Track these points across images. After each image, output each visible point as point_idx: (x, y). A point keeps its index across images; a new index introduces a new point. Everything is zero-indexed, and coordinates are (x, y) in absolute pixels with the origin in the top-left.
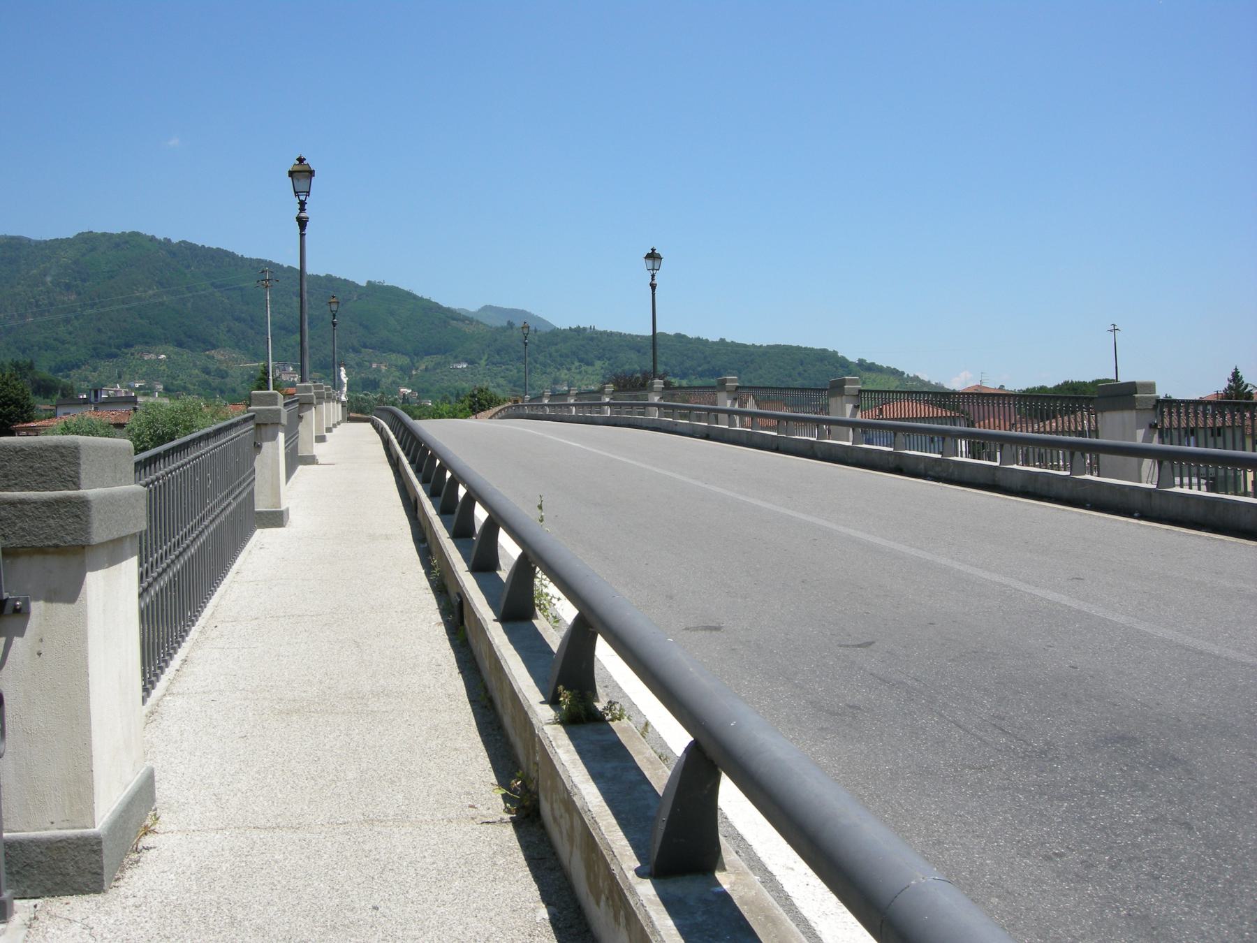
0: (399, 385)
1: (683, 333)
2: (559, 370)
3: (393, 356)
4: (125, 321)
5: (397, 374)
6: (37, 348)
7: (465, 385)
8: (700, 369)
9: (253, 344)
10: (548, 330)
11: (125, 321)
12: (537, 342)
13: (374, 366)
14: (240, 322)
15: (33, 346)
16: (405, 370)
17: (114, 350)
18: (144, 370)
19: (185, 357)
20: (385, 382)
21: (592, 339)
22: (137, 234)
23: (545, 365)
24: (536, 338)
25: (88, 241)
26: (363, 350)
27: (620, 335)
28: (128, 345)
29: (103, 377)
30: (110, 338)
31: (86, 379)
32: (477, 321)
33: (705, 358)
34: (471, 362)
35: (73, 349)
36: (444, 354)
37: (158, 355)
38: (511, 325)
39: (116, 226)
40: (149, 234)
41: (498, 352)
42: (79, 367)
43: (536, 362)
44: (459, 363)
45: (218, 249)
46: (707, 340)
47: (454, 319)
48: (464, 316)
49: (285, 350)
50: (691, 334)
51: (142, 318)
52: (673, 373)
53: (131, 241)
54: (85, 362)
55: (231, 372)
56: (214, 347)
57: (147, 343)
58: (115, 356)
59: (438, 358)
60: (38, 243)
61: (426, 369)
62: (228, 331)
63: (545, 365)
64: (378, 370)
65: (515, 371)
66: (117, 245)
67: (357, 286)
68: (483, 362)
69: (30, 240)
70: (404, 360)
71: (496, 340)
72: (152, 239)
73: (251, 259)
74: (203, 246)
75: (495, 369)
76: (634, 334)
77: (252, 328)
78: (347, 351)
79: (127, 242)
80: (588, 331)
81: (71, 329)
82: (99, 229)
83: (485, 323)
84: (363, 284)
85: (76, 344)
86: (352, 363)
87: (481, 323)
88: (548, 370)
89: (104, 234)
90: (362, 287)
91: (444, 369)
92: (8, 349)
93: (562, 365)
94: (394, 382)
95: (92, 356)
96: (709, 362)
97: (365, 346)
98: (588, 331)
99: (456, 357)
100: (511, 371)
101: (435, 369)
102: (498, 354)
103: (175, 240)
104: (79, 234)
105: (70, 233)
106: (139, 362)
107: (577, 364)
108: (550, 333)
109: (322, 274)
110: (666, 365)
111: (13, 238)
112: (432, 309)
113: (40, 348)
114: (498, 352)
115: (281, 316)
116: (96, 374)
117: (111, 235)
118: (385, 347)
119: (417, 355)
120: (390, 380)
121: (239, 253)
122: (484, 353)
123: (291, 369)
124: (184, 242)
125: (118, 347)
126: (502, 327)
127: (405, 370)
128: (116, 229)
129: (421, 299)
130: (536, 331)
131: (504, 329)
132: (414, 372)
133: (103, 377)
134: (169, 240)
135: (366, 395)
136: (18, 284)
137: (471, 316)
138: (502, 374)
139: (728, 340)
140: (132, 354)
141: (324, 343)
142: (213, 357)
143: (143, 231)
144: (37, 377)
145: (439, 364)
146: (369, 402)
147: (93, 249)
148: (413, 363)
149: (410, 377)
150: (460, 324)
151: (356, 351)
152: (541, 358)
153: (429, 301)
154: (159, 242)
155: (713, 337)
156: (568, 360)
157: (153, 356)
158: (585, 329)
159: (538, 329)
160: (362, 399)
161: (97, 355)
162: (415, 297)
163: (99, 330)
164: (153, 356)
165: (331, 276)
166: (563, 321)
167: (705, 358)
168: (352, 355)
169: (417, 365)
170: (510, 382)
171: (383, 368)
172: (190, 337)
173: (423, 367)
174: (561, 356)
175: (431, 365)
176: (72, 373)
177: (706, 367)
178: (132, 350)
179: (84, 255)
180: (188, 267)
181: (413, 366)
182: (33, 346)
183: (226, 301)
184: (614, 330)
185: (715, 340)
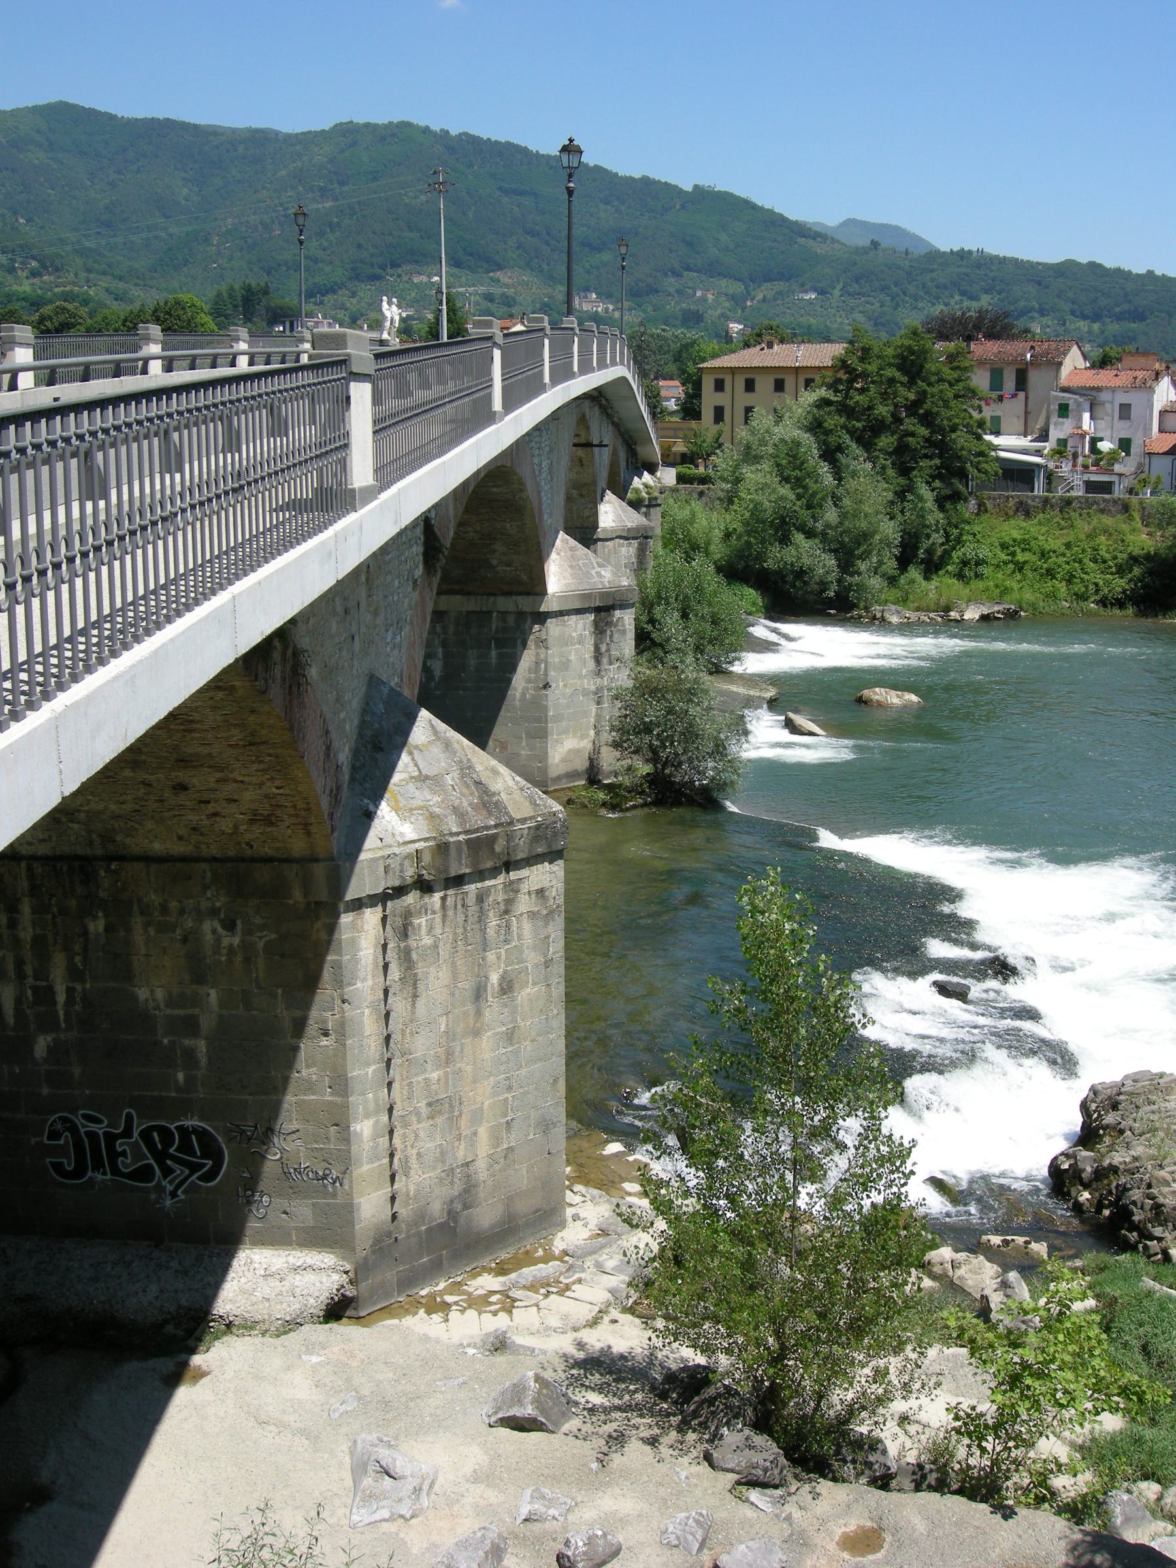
0: (728, 319)
1: (1098, 261)
2: (934, 304)
3: (723, 282)
4: (390, 234)
5: (727, 304)
6: (284, 268)
7: (812, 321)
8: (1117, 310)
9: (548, 264)
10: (924, 251)
11: (390, 234)
12: (907, 268)
13: (699, 294)
14: (533, 236)
15: (279, 265)
16: (738, 301)
17: (378, 271)
18: (413, 295)
19: (463, 279)
20: (712, 314)
21: (978, 266)
22: (407, 125)
23: (916, 298)
24: (907, 263)
25: (347, 132)
26: (685, 273)
27: (1016, 262)
28: (394, 265)
29: (363, 304)
30: (372, 255)
31: (343, 307)
32: (833, 239)
33: (1126, 295)
34: (822, 292)
35: (328, 269)
36: (788, 280)
37: (430, 276)
38: (875, 244)
39: (381, 115)
40: (422, 124)
41: (857, 279)
42: (334, 292)
43: (904, 293)
44: (806, 292)
45: (508, 143)
46: (1130, 272)
47: (803, 236)
48: (816, 232)
49: (588, 272)
50: (1109, 263)
51: (411, 231)
52: (1082, 313)
53: (400, 133)
54: (342, 286)
55: (520, 299)
56: (500, 267)
57: (417, 262)
58: (378, 278)
59: (780, 286)
60: (289, 136)
61: (764, 300)
62: (518, 248)
63: (916, 298)
64: (704, 299)
65: (878, 305)
66: (383, 138)
67: (680, 191)
68: (837, 293)
69: (277, 133)
70: (737, 288)
71: (855, 264)
72: (426, 130)
73: (548, 156)
74: (489, 139)
75: (852, 302)
76: (1035, 260)
77: (548, 244)
78: (665, 275)
79: (394, 135)
80: (975, 254)
81: (325, 244)
82: (360, 119)
83: (842, 241)
84: (688, 187)
85: (331, 263)
86: (671, 290)
87: (838, 242)
88: (920, 305)
89: (367, 125)
90: (686, 193)
91: (787, 300)
92: (251, 270)
93: (937, 298)
94: (723, 315)
95: (350, 278)
96: (1130, 302)
97: (688, 269)
98: (975, 254)
99: (803, 285)
100: (872, 304)
101: (776, 300)
102: (857, 282)
103: (454, 132)
104: (336, 125)
105: (324, 123)
106: (407, 286)
107: (957, 297)
108: (925, 256)
109: (637, 175)
110: (1073, 303)
111: (257, 131)
112: (774, 222)
113: (288, 268)
114: (857, 279)
115: (585, 229)
116: (354, 301)
117: (376, 125)
118: (713, 270)
119: (753, 281)
120: (719, 312)
121: (533, 148)
122: (838, 280)
123: (594, 296)
124: (465, 134)
125: (383, 267)
126: (863, 248)
127: (738, 301)
128: (381, 117)
129: (762, 209)
130: (907, 253)
131: (863, 251)
132: (749, 303)
133: (363, 304)
134: (447, 132)
135: (663, 330)
136: (263, 188)
137: (824, 232)
138: (861, 308)
139: (1158, 273)
140: (399, 276)
141: (637, 264)
142: (499, 281)
143: (415, 121)
144: (273, 305)
145: (780, 293)
146: (665, 339)
147: (354, 144)
148: (748, 293)
149: (744, 309)
150: (811, 242)
151: (676, 274)
152: (911, 289)
153: (771, 212)
154: (434, 134)
155: (1139, 269)
156: (947, 293)
157: (424, 279)
158: (970, 252)
159: (910, 250)
160: (658, 336)
161: (357, 277)
162: (753, 207)
163: (359, 246)
164: (424, 279)
165: (648, 178)
166: (946, 243)
167: (1126, 295)
168: (672, 280)
169: (753, 293)
170: (870, 319)
171: (710, 296)
172: (471, 255)
173: (761, 297)
174: (937, 287)
175: (770, 295)
176: (326, 299)
177: (1126, 307)
178: (399, 270)
179: (342, 151)
180: (470, 166)
181: (748, 295)
182: (279, 265)
183: (516, 209)
184: (1009, 255)
185: (1140, 272)
